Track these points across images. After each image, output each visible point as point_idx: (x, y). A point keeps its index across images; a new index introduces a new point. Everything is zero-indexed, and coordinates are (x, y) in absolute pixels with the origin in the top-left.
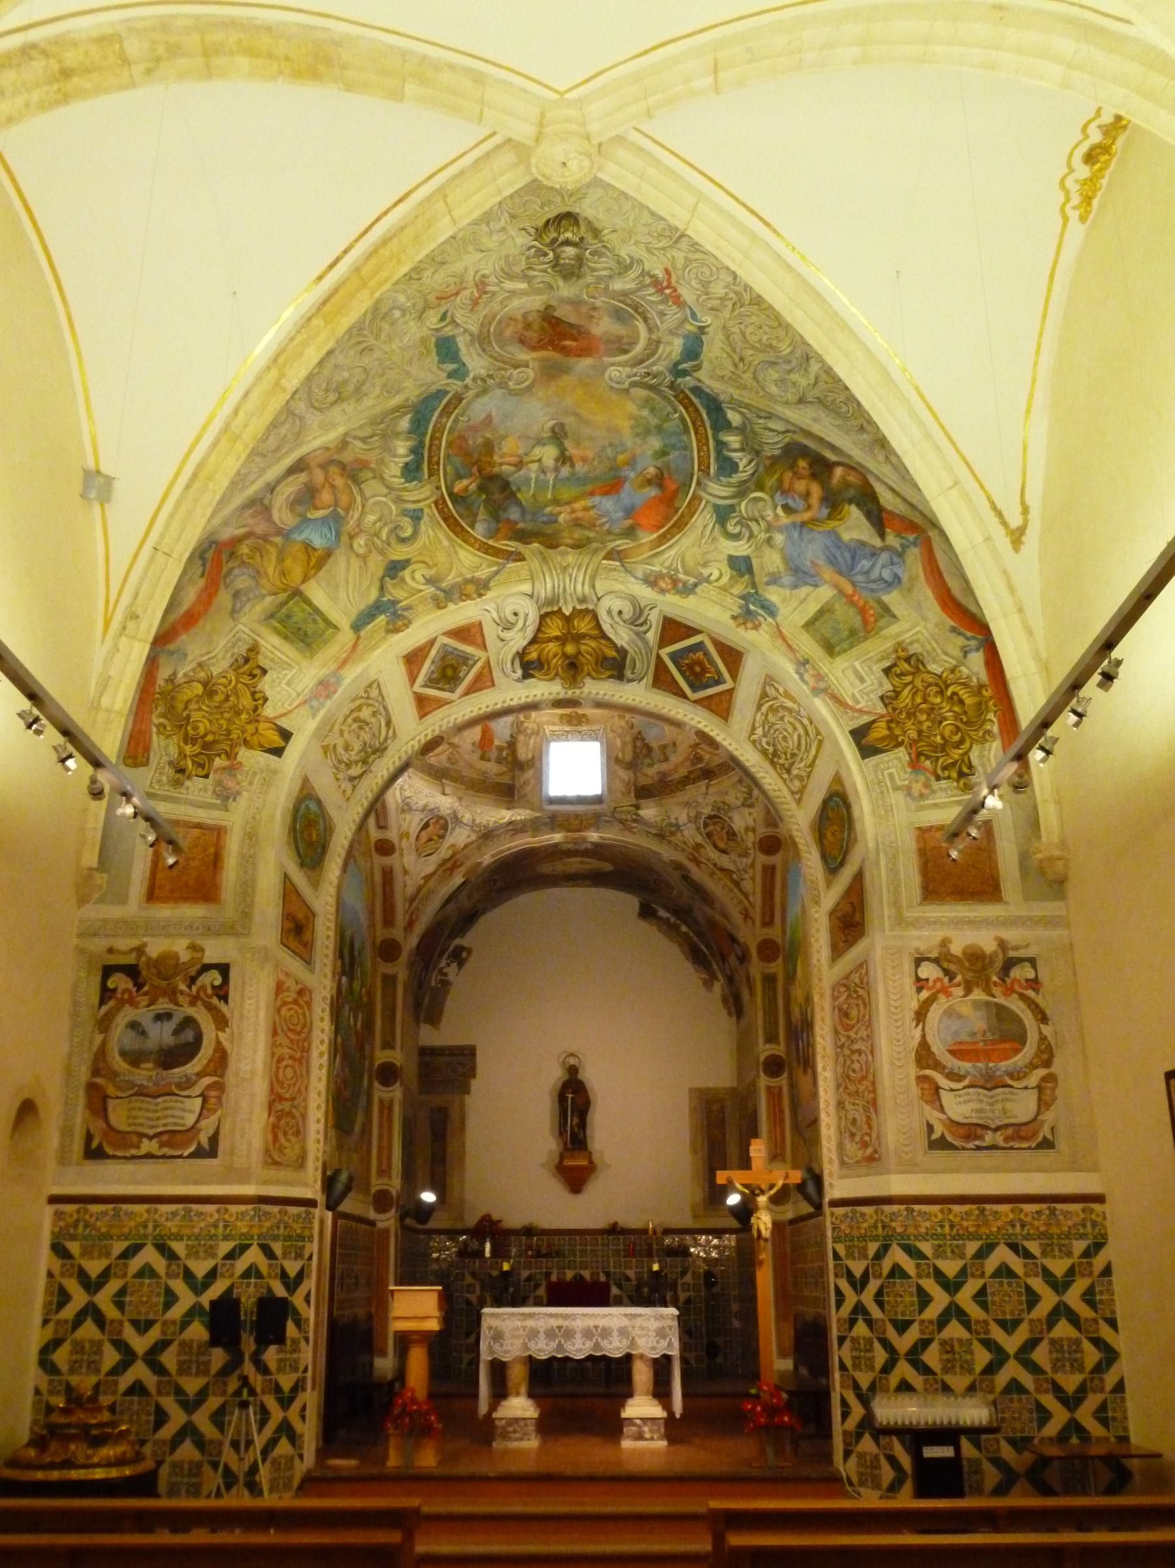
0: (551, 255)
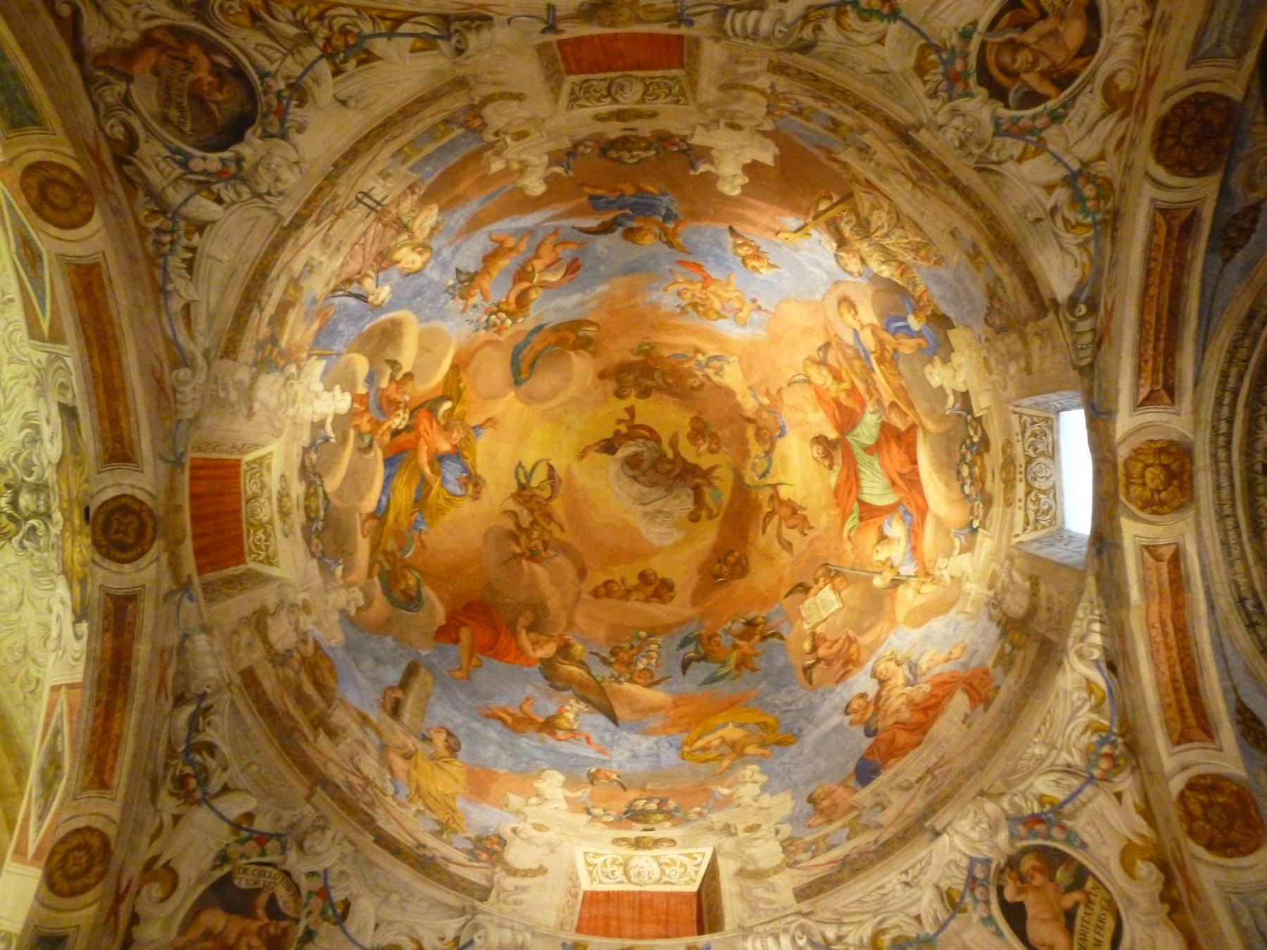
0: (34, 522)
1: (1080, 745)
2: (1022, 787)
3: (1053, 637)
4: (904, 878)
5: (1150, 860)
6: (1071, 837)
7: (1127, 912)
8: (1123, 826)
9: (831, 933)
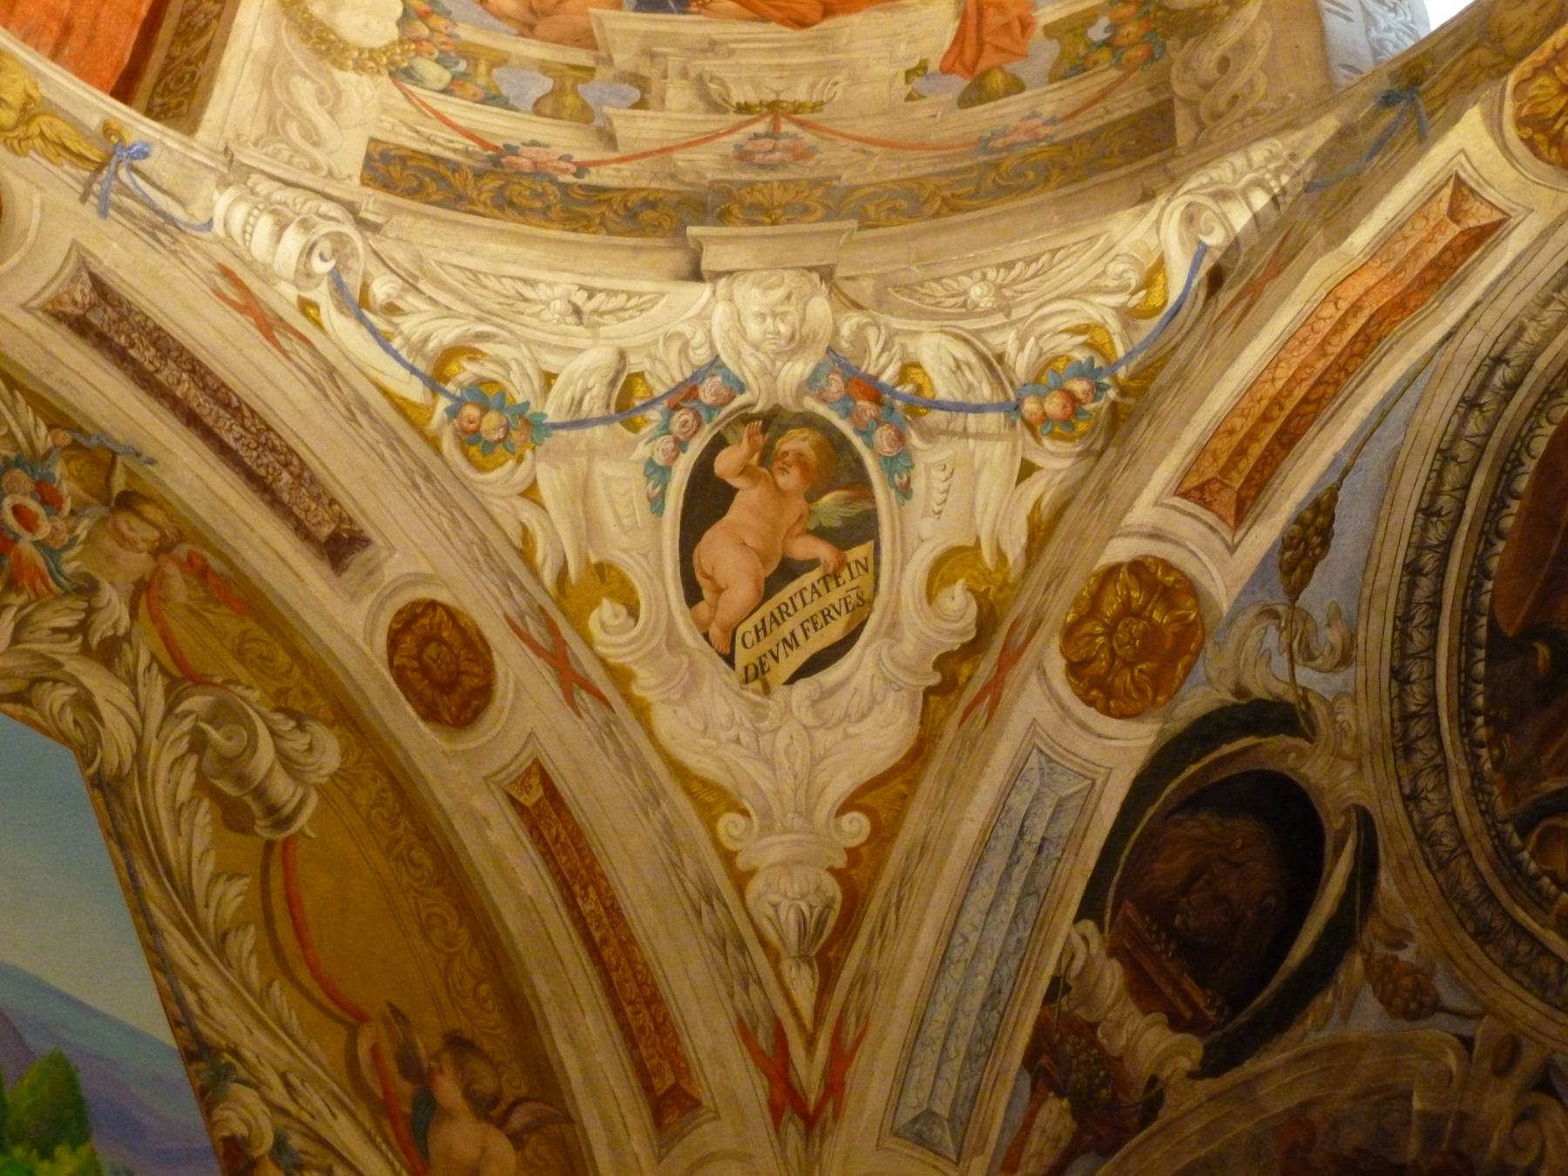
1: (1047, 345)
2: (897, 323)
3: (1184, 132)
4: (580, 298)
5: (980, 597)
6: (899, 462)
7: (875, 635)
8: (989, 518)
9: (382, 288)
